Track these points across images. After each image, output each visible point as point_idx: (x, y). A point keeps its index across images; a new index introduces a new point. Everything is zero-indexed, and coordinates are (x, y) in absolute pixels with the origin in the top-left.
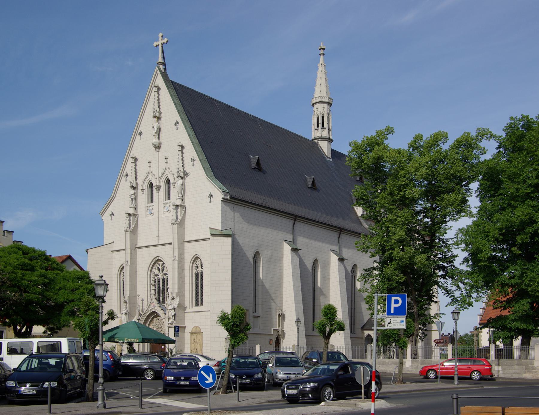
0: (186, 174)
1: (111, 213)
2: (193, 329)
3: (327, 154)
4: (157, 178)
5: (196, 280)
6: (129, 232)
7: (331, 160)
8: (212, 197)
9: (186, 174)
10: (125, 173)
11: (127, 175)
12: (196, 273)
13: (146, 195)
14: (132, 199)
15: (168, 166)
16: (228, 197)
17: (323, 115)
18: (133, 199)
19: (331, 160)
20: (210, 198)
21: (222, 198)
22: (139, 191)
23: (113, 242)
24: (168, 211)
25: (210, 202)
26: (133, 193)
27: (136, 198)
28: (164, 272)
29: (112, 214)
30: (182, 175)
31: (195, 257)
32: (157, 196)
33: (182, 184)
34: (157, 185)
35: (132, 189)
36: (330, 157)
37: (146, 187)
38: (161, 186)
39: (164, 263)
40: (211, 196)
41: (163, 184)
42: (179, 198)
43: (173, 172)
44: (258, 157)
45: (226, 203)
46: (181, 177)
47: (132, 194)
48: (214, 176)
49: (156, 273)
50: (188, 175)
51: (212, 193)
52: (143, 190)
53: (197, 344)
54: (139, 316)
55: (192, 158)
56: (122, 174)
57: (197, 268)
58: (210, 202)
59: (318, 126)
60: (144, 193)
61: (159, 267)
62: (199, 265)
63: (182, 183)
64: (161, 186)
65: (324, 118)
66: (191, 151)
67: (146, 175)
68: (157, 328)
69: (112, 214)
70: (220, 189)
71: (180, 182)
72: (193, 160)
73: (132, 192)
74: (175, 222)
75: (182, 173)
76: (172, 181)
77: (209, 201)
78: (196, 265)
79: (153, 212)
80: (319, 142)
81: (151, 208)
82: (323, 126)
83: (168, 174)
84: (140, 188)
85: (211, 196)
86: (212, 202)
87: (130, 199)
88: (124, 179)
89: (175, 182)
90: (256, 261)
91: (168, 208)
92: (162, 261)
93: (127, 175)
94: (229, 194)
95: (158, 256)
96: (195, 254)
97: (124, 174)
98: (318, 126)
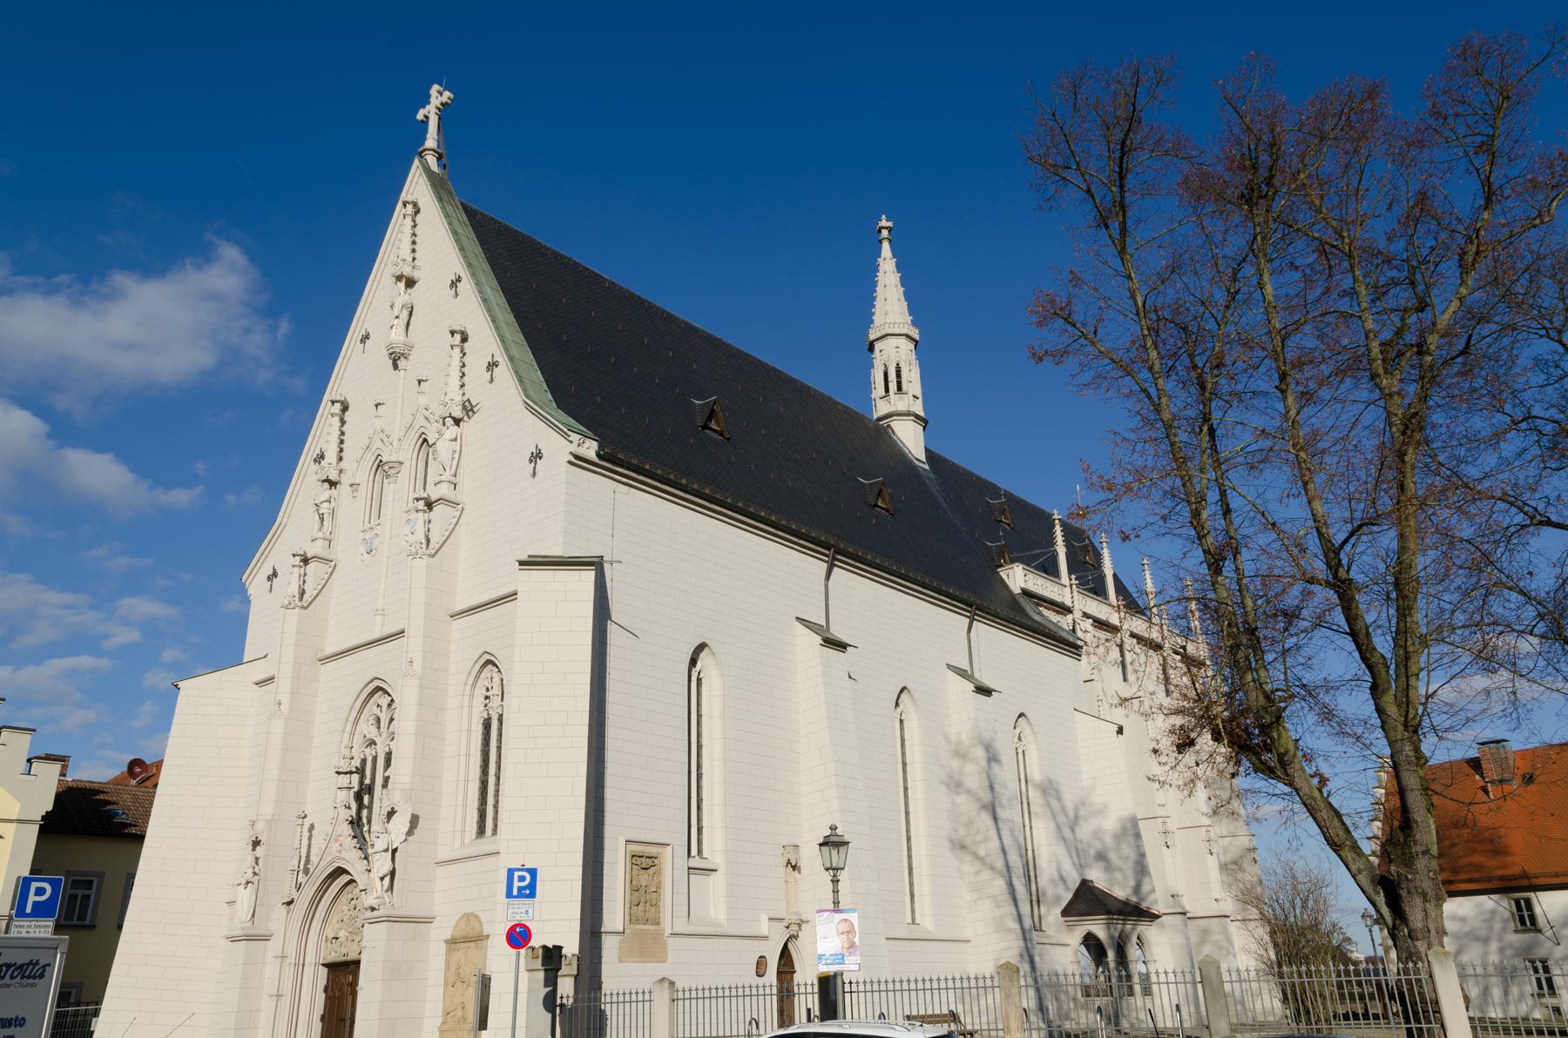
0: (469, 409)
1: (271, 572)
2: (457, 923)
3: (913, 452)
6: (297, 609)
7: (927, 467)
8: (540, 458)
9: (469, 409)
12: (485, 720)
17: (898, 364)
19: (927, 467)
20: (533, 464)
25: (534, 474)
26: (327, 498)
29: (275, 574)
30: (458, 413)
31: (482, 662)
33: (456, 440)
35: (326, 485)
36: (925, 460)
39: (392, 700)
40: (537, 456)
42: (443, 478)
46: (454, 419)
49: (368, 736)
50: (474, 412)
51: (539, 447)
53: (465, 985)
54: (294, 890)
58: (534, 474)
59: (887, 390)
62: (496, 690)
63: (453, 436)
65: (900, 371)
66: (486, 341)
68: (350, 930)
69: (275, 574)
70: (563, 424)
72: (492, 366)
74: (420, 552)
77: (532, 469)
78: (488, 690)
80: (891, 423)
81: (368, 536)
82: (899, 388)
85: (537, 456)
90: (699, 680)
92: (389, 695)
96: (481, 652)
97: (315, 456)
98: (887, 390)
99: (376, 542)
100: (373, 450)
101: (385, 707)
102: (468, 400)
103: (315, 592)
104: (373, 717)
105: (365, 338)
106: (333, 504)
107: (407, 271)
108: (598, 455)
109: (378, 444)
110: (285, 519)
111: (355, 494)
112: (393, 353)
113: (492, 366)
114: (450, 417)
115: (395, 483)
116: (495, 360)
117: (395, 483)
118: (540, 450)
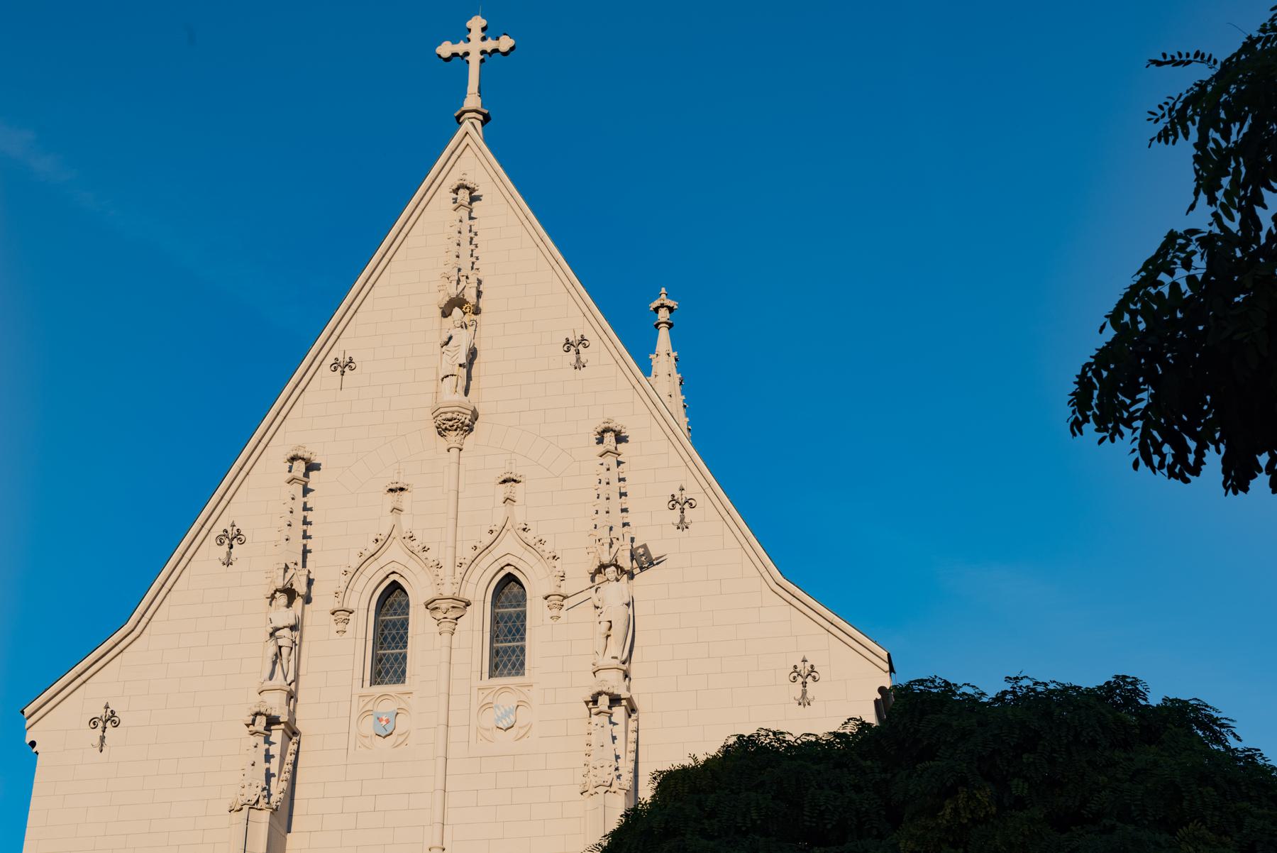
0: (644, 560)
4: (448, 564)
9: (644, 560)
13: (361, 643)
15: (519, 515)
22: (317, 616)
27: (295, 645)
32: (446, 651)
34: (447, 594)
37: (363, 600)
38: (468, 604)
41: (480, 596)
43: (548, 548)
52: (342, 614)
67: (373, 547)
71: (614, 592)
73: (283, 616)
76: (536, 584)
79: (402, 723)
83: (518, 549)
84: (323, 598)
88: (212, 552)
89: (563, 591)
93: (232, 538)
97: (218, 530)
105: (344, 366)
115: (453, 634)
116: (687, 495)
118: (812, 667)
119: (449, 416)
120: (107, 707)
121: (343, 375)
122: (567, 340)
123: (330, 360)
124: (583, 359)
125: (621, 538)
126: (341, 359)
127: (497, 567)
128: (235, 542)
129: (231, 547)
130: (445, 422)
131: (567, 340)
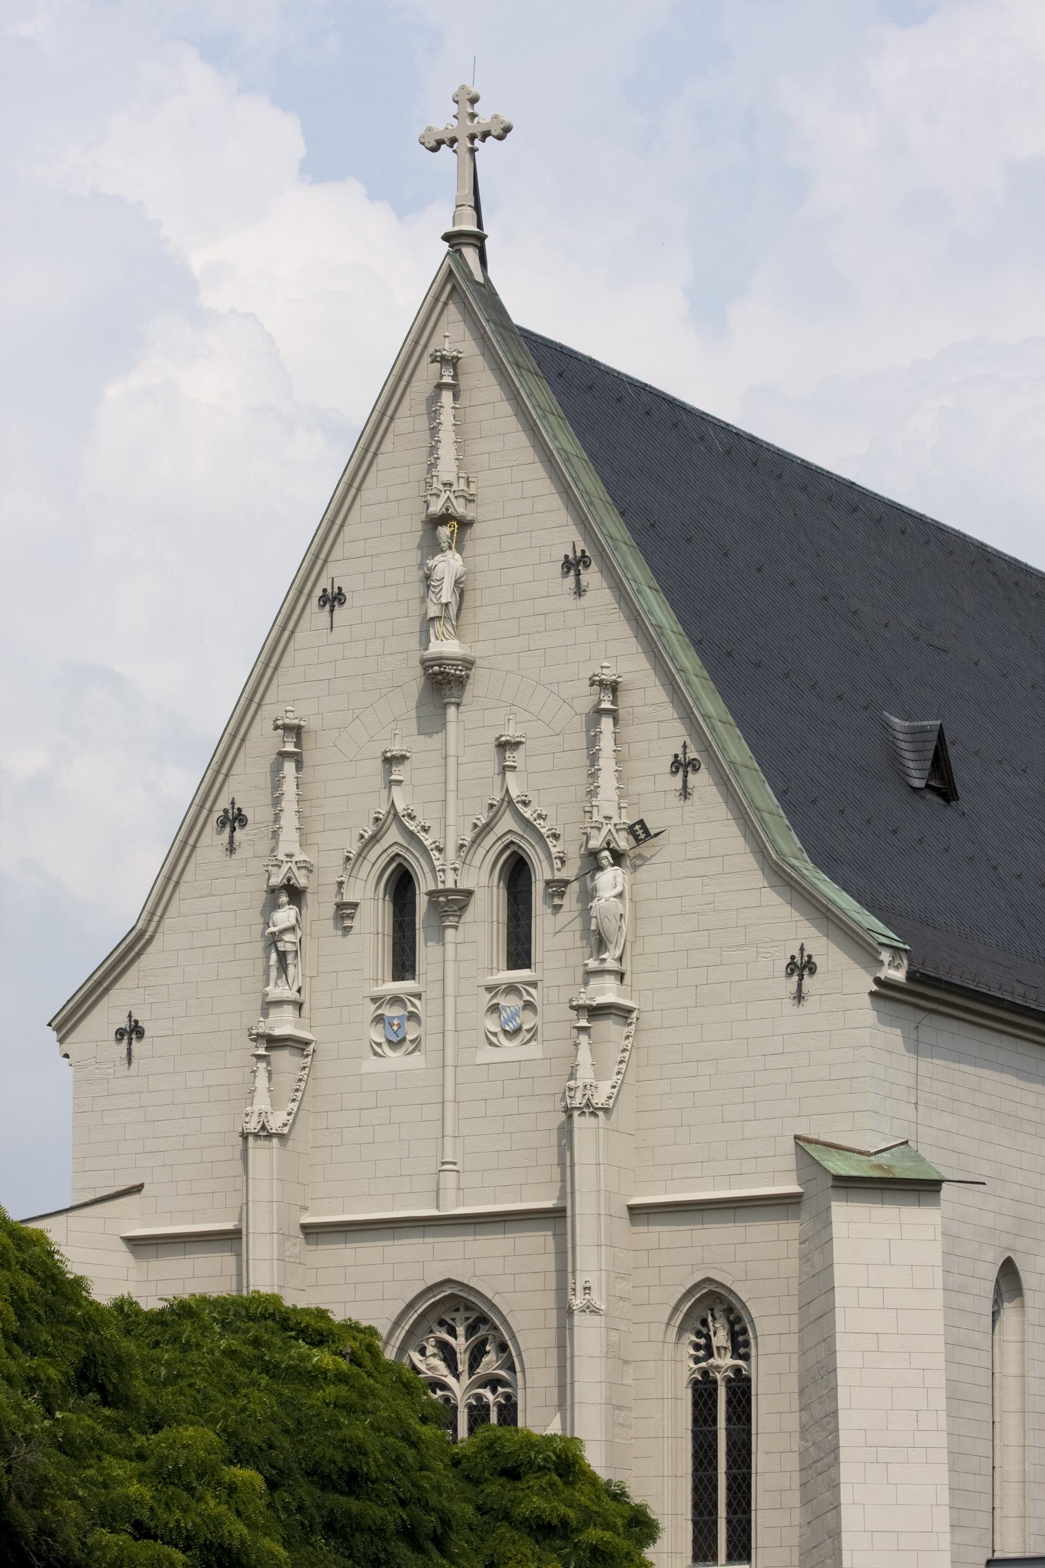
1: (124, 1024)
5: (695, 1421)
10: (223, 803)
11: (234, 819)
12: (695, 1383)
14: (282, 956)
16: (899, 975)
18: (290, 959)
21: (878, 981)
23: (138, 1189)
24: (518, 1030)
26: (293, 921)
28: (480, 1370)
29: (132, 1032)
34: (450, 885)
35: (284, 899)
44: (939, 722)
45: (890, 1007)
47: (287, 924)
48: (806, 856)
55: (679, 751)
56: (205, 812)
57: (701, 1353)
60: (355, 923)
61: (450, 1340)
62: (721, 1338)
64: (469, 893)
69: (132, 1032)
75: (623, 834)
86: (811, 1004)
87: (274, 957)
91: (512, 1018)
94: (904, 956)
95: (449, 1282)
97: (218, 814)
99: (411, 1031)
100: (385, 842)
101: (460, 1330)
102: (641, 822)
103: (294, 1106)
104: (432, 1341)
105: (333, 599)
106: (299, 933)
107: (460, 508)
108: (910, 976)
109: (393, 835)
110: (153, 924)
111: (348, 923)
112: (441, 673)
113: (681, 766)
114: (608, 849)
117: (456, 928)
119: (436, 668)
120: (130, 1016)
121: (332, 611)
122: (566, 557)
123: (318, 592)
124: (584, 583)
125: (614, 813)
126: (329, 590)
127: (499, 846)
128: (236, 824)
129: (233, 829)
130: (433, 676)
131: (566, 557)
